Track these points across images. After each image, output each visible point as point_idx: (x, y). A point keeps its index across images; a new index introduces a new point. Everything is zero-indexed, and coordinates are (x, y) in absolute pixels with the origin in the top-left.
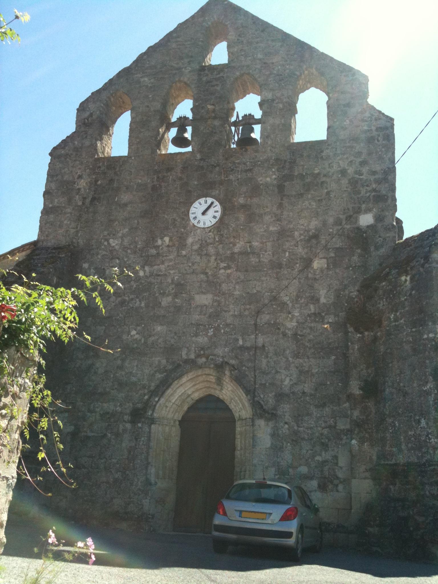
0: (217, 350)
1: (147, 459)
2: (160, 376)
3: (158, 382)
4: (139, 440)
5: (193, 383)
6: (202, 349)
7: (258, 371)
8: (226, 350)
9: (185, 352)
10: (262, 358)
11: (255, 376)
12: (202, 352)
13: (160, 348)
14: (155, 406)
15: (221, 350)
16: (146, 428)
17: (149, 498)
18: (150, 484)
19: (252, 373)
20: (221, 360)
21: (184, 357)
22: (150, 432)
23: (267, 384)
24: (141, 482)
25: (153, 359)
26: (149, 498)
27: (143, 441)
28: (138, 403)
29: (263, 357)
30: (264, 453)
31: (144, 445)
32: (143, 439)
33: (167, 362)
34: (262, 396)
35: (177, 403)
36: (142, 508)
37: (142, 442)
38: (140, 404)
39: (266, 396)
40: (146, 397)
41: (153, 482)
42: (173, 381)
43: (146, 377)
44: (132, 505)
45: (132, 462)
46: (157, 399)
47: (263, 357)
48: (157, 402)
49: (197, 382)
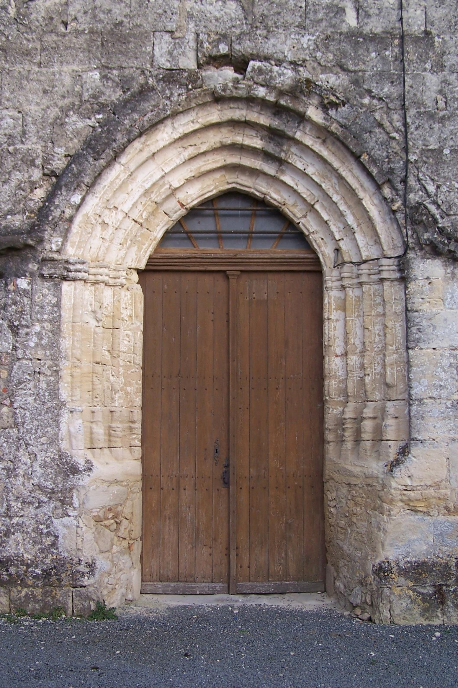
0: (272, 41)
2: (80, 125)
4: (23, 331)
5: (191, 151)
6: (223, 37)
7: (412, 112)
8: (306, 40)
9: (165, 48)
10: (425, 70)
11: (405, 125)
12: (223, 49)
13: (78, 33)
14: (71, 220)
15: (289, 42)
16: (46, 291)
17: (75, 513)
18: (74, 470)
19: (396, 117)
20: (289, 73)
21: (164, 62)
23: (446, 151)
24: (44, 465)
25: (56, 69)
27: (39, 335)
28: (10, 212)
29: (428, 66)
30: (445, 362)
31: (44, 347)
32: (37, 328)
33: (104, 77)
34: (431, 188)
35: (135, 215)
36: (54, 544)
38: (19, 217)
39: (444, 189)
40: (40, 193)
41: (81, 463)
42: (130, 142)
43: (32, 128)
44: (19, 536)
45: (7, 402)
46: (76, 198)
47: (428, 66)
48: (78, 207)
49: (204, 148)
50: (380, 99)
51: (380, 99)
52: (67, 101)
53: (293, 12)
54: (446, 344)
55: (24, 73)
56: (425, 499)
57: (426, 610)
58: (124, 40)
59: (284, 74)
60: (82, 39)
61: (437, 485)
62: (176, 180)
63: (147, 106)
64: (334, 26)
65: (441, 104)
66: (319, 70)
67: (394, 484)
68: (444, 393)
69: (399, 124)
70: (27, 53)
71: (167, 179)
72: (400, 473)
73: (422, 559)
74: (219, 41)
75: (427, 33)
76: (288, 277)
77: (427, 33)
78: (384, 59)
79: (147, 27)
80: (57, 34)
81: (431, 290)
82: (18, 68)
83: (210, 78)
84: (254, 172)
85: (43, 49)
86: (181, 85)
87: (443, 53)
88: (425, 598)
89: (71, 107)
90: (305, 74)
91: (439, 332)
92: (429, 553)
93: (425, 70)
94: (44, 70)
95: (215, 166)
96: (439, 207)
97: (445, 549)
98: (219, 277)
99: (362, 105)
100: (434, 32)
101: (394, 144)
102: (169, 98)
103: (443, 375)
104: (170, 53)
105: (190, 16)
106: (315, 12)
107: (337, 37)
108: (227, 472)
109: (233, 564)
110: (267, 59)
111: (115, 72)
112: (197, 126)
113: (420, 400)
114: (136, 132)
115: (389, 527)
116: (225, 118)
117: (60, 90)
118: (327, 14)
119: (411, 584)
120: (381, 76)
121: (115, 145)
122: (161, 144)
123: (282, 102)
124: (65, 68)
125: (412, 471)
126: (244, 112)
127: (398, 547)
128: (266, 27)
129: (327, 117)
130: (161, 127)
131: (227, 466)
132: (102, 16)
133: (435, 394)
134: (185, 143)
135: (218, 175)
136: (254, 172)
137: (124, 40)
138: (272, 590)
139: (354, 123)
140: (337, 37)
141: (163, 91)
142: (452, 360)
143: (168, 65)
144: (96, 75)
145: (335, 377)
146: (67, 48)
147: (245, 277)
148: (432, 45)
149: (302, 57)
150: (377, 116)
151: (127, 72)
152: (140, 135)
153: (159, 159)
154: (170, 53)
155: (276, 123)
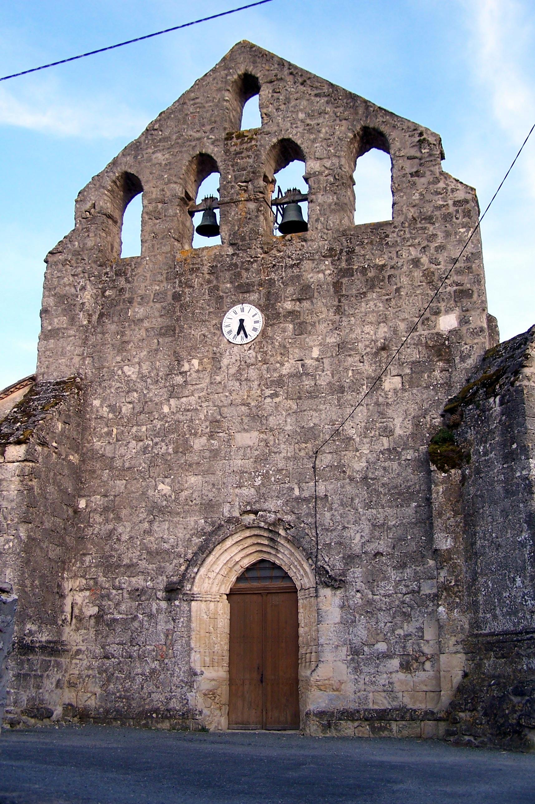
0: (267, 504)
1: (188, 644)
2: (197, 541)
3: (195, 548)
4: (177, 621)
5: (241, 547)
6: (249, 503)
7: (320, 528)
8: (279, 502)
9: (228, 509)
10: (325, 511)
11: (317, 534)
12: (249, 508)
13: (196, 505)
14: (194, 578)
15: (273, 504)
16: (185, 606)
17: (195, 691)
18: (195, 674)
19: (313, 531)
20: (273, 516)
21: (227, 514)
22: (190, 611)
23: (333, 544)
24: (184, 672)
25: (188, 519)
26: (195, 691)
27: (182, 622)
28: (172, 576)
29: (326, 509)
30: (332, 630)
31: (184, 627)
32: (182, 620)
33: (206, 522)
34: (327, 559)
35: (222, 573)
36: (187, 703)
37: (181, 624)
38: (175, 577)
39: (332, 559)
40: (183, 568)
41: (199, 671)
42: (214, 547)
43: (180, 542)
44: (174, 700)
45: (171, 648)
46: (196, 570)
47: (326, 509)
48: (197, 573)
49: (246, 546)
50: (307, 524)
51: (307, 524)
52: (192, 532)
53: (274, 491)
54: (332, 622)
55: (177, 521)
56: (324, 685)
57: (323, 730)
58: (212, 506)
59: (271, 517)
60: (198, 507)
61: (329, 679)
62: (237, 558)
63: (220, 533)
64: (290, 496)
65: (331, 524)
66: (284, 514)
67: (312, 679)
68: (331, 642)
69: (314, 534)
70: (178, 514)
71: (233, 558)
72: (314, 674)
73: (324, 710)
74: (247, 505)
75: (326, 495)
76: (287, 595)
77: (326, 495)
78: (309, 507)
79: (221, 501)
80: (189, 506)
81: (326, 601)
82: (175, 519)
83: (245, 519)
84: (269, 553)
85: (184, 512)
86: (233, 523)
87: (332, 503)
88: (323, 725)
89: (194, 534)
90: (279, 516)
91: (329, 617)
92: (326, 707)
93: (325, 511)
94: (184, 520)
95: (252, 551)
96: (330, 567)
97: (332, 706)
98: (260, 596)
99: (301, 527)
100: (328, 495)
101: (313, 542)
102: (228, 529)
103: (331, 635)
104: (229, 511)
105: (237, 495)
106: (283, 491)
107: (291, 500)
108: (262, 677)
109: (264, 716)
110: (265, 511)
111: (210, 519)
112: (241, 538)
113: (322, 645)
114: (217, 543)
115: (310, 696)
116: (252, 534)
117: (190, 527)
118: (287, 491)
119: (318, 719)
120: (308, 515)
121: (209, 549)
122: (228, 546)
123: (270, 528)
124: (192, 519)
125: (319, 674)
126: (259, 532)
127: (314, 705)
128: (265, 498)
129: (287, 534)
130: (227, 540)
131: (262, 675)
132: (205, 497)
133: (328, 642)
134: (238, 544)
135: (256, 554)
136: (269, 553)
137: (212, 506)
138: (280, 728)
139: (297, 535)
140: (291, 500)
141: (226, 526)
142: (334, 629)
143: (229, 516)
144: (203, 521)
145: (302, 636)
146: (192, 511)
147: (269, 595)
148: (328, 500)
149: (278, 509)
150: (306, 531)
151: (213, 519)
152: (219, 544)
153: (229, 551)
154: (229, 511)
155: (270, 535)
